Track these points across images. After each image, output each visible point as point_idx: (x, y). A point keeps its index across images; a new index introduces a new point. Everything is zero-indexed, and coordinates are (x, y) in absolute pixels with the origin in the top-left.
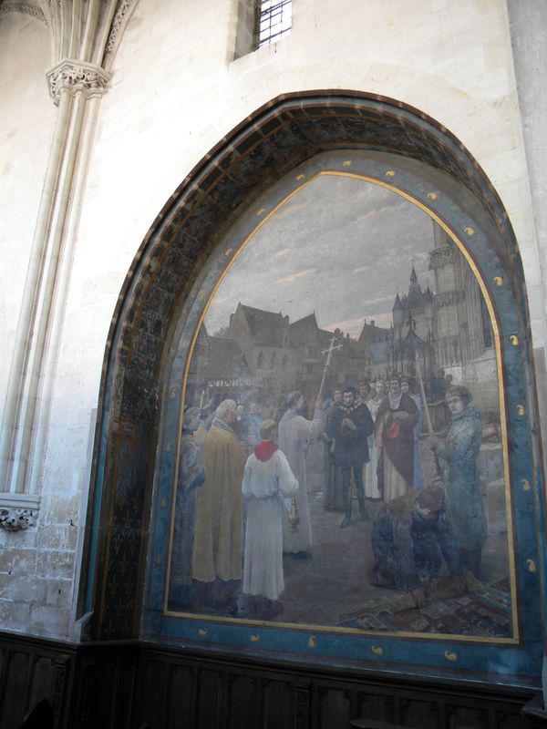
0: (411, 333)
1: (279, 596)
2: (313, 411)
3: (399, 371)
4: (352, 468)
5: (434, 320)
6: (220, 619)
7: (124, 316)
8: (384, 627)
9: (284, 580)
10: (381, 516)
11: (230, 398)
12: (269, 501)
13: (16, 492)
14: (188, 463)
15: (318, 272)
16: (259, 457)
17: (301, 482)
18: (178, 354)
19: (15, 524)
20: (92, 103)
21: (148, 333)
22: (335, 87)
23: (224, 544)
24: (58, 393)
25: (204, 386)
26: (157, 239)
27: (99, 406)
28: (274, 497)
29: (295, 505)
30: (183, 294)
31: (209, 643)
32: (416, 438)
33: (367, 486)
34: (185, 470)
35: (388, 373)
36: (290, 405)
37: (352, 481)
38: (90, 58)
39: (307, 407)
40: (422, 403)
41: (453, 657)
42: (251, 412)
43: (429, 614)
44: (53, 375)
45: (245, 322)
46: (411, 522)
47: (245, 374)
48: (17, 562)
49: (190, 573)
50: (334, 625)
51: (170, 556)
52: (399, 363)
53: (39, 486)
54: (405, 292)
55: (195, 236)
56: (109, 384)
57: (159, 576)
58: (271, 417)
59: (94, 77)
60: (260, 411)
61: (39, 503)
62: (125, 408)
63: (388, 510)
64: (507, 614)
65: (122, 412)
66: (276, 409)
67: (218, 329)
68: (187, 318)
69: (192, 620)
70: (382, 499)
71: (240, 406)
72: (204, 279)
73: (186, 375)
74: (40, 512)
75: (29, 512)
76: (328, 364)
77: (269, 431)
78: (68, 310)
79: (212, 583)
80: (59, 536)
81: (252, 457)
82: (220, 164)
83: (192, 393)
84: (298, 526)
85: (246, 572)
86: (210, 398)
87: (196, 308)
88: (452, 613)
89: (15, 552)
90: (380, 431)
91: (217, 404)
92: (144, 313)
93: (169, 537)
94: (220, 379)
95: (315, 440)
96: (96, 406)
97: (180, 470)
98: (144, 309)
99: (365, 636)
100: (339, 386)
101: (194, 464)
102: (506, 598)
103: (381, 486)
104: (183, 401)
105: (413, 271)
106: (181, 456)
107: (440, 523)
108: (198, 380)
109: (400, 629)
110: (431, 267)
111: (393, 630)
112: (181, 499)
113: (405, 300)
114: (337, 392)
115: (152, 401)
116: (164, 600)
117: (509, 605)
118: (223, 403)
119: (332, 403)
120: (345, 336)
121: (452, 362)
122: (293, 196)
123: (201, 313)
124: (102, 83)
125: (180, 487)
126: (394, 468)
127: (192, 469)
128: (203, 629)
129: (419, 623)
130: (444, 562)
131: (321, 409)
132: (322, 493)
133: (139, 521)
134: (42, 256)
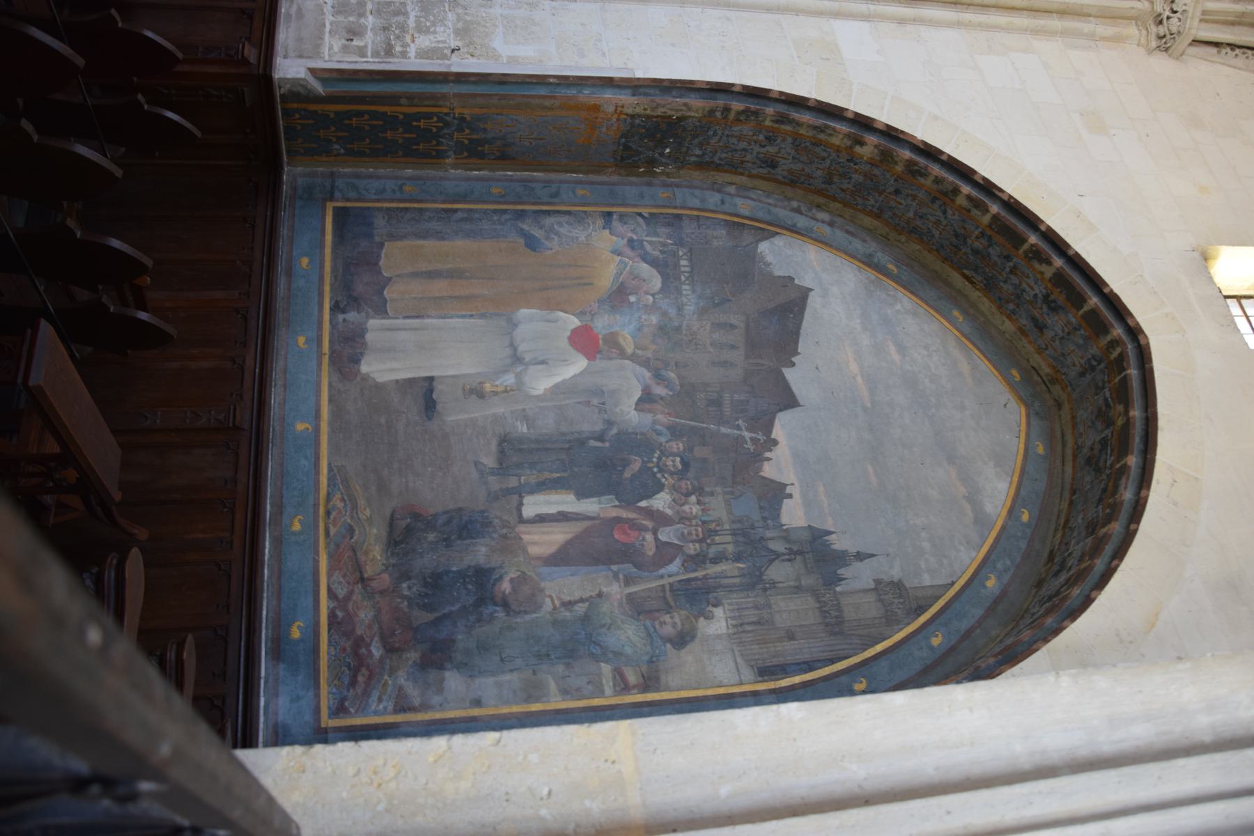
0: (777, 556)
1: (367, 374)
2: (650, 411)
3: (717, 538)
4: (565, 474)
5: (798, 589)
6: (327, 288)
7: (782, 108)
8: (333, 531)
9: (391, 381)
10: (496, 520)
11: (663, 283)
12: (508, 351)
14: (560, 224)
16: (574, 332)
17: (538, 398)
18: (727, 199)
20: (1132, 30)
21: (757, 149)
22: (1161, 422)
23: (440, 287)
25: (680, 243)
26: (907, 154)
28: (517, 359)
29: (506, 391)
30: (821, 200)
31: (289, 274)
32: (614, 568)
33: (540, 498)
34: (548, 221)
35: (712, 521)
36: (658, 377)
37: (547, 475)
38: (1207, 18)
39: (655, 401)
40: (670, 576)
41: (296, 634)
42: (644, 317)
43: (354, 598)
46: (488, 566)
49: (392, 237)
50: (328, 458)
51: (416, 205)
52: (729, 538)
54: (839, 543)
55: (916, 214)
57: (384, 190)
58: (637, 347)
59: (1174, 30)
60: (646, 330)
62: (637, 121)
63: (505, 531)
64: (362, 710)
65: (633, 116)
66: (649, 354)
67: (769, 258)
68: (784, 208)
69: (322, 246)
70: (522, 520)
71: (650, 298)
72: (848, 232)
73: (695, 213)
76: (724, 430)
79: (381, 273)
80: (435, 32)
81: (574, 322)
82: (1032, 245)
83: (669, 225)
84: (473, 397)
85: (400, 322)
87: (802, 222)
88: (359, 632)
90: (625, 514)
91: (654, 263)
92: (790, 140)
93: (444, 202)
94: (692, 266)
95: (606, 416)
96: (640, 74)
97: (548, 213)
98: (795, 140)
99: (316, 505)
100: (690, 449)
101: (557, 234)
102: (385, 708)
103: (541, 519)
105: (872, 556)
107: (491, 608)
108: (689, 228)
109: (330, 556)
110: (878, 582)
111: (327, 545)
112: (507, 216)
113: (827, 545)
114: (681, 446)
115: (652, 162)
117: (376, 713)
118: (654, 272)
119: (663, 439)
120: (767, 455)
121: (732, 618)
122: (984, 365)
123: (793, 230)
124: (1165, 44)
126: (569, 536)
129: (340, 583)
130: (431, 616)
131: (655, 422)
132: (525, 430)
133: (466, 154)
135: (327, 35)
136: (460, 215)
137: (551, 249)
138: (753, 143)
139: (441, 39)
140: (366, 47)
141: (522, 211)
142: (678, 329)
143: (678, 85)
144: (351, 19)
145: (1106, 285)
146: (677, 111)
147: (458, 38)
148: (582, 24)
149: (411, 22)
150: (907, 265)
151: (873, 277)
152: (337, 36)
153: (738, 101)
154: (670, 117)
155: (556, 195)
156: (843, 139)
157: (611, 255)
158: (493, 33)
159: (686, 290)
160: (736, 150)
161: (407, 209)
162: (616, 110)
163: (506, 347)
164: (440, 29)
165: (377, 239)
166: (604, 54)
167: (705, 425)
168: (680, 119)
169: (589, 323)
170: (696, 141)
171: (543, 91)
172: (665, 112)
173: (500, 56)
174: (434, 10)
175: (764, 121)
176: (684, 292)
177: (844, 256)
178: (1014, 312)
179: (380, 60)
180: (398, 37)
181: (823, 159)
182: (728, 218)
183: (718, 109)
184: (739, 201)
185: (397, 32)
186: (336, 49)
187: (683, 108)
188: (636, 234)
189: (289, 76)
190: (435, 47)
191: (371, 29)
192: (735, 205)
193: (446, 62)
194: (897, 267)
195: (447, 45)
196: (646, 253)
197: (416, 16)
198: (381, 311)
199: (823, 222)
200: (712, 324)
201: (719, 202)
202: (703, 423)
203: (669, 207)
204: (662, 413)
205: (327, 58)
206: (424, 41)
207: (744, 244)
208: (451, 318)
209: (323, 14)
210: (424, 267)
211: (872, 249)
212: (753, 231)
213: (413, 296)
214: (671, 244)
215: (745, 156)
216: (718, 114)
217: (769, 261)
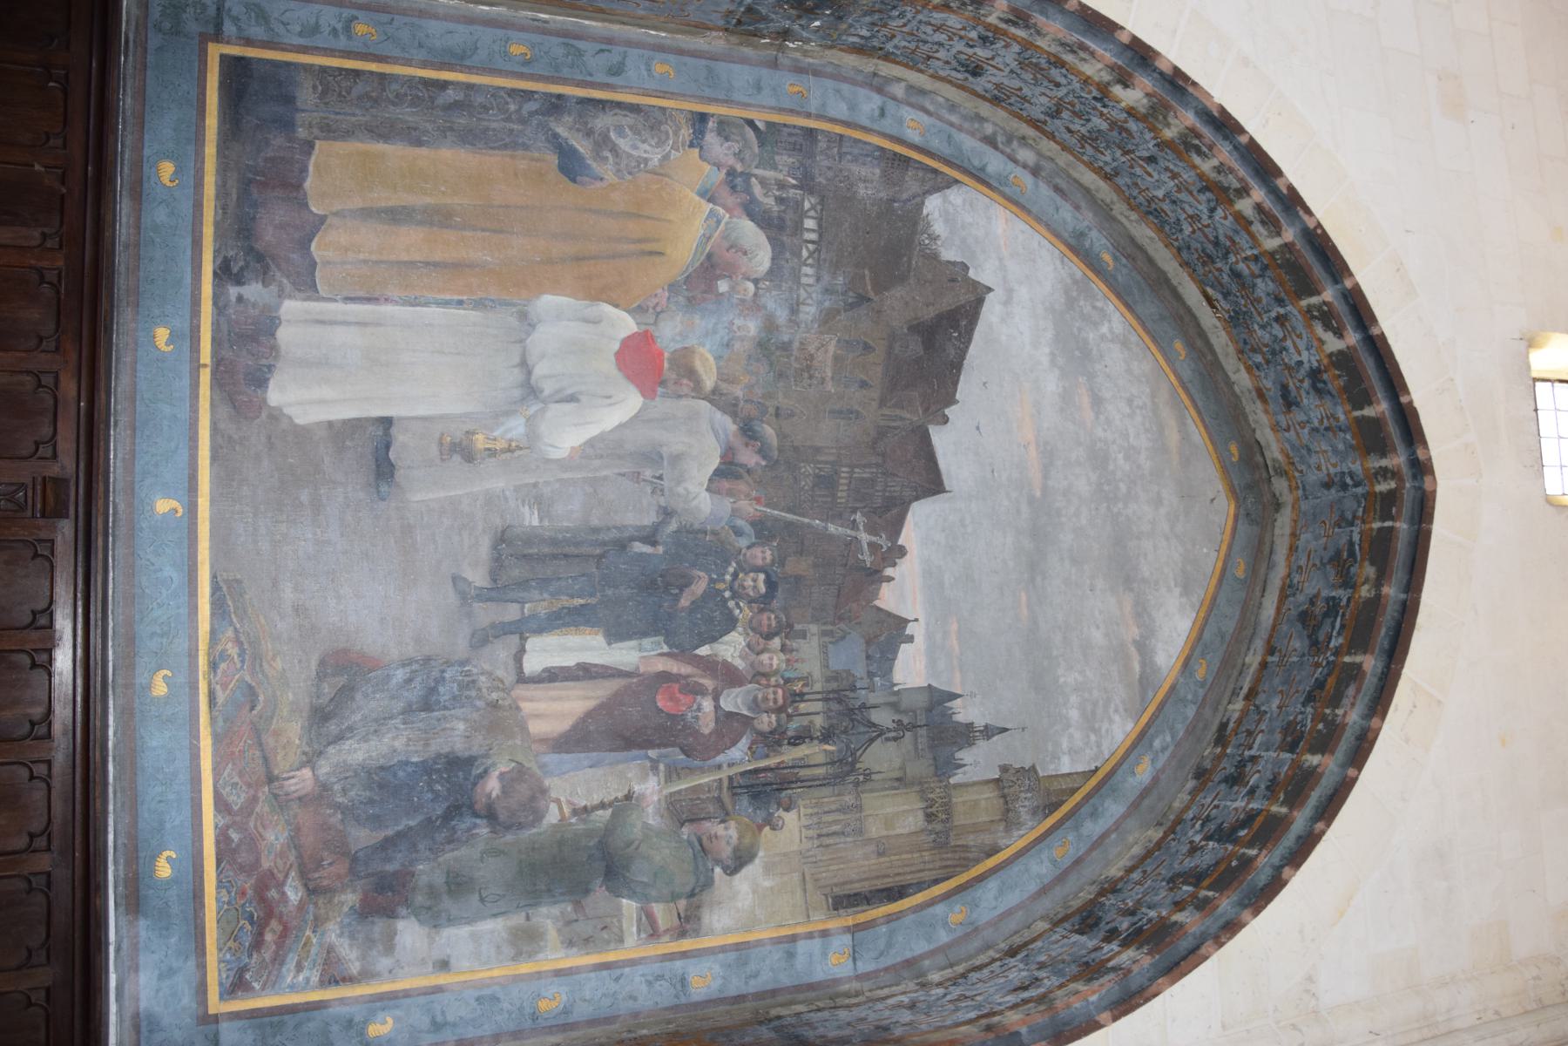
0: (879, 732)
1: (279, 409)
2: (730, 493)
3: (802, 705)
4: (592, 601)
5: (901, 781)
6: (208, 231)
8: (221, 697)
9: (318, 424)
10: (483, 678)
12: (517, 375)
14: (620, 130)
15: (1031, 500)
16: (626, 343)
17: (563, 464)
18: (891, 106)
22: (1422, 618)
23: (409, 241)
25: (807, 184)
28: (530, 391)
29: (509, 450)
31: (137, 194)
32: (652, 753)
33: (551, 640)
34: (602, 122)
35: (800, 679)
36: (748, 431)
37: (565, 601)
39: (738, 477)
40: (730, 765)
41: (164, 870)
42: (738, 322)
43: (258, 809)
45: (947, 303)
46: (467, 754)
47: (827, 304)
49: (330, 131)
50: (212, 567)
51: (373, 67)
52: (818, 706)
54: (966, 712)
55: (1167, 195)
57: (315, 29)
58: (722, 377)
60: (737, 345)
63: (494, 696)
64: (271, 985)
66: (739, 392)
67: (938, 227)
68: (972, 134)
69: (199, 141)
70: (522, 679)
71: (751, 286)
73: (838, 129)
76: (832, 528)
77: (691, 373)
79: (306, 205)
81: (627, 325)
83: (795, 148)
84: (457, 458)
85: (337, 308)
86: (780, 200)
88: (266, 864)
90: (674, 667)
91: (765, 221)
93: (424, 65)
94: (821, 230)
95: (662, 501)
97: (602, 105)
99: (193, 655)
100: (781, 561)
101: (614, 150)
102: (308, 980)
104: (776, 118)
105: (1005, 730)
106: (635, 109)
107: (469, 821)
109: (217, 738)
110: (1004, 769)
111: (213, 720)
112: (532, 106)
113: (947, 715)
114: (768, 553)
116: (249, 42)
117: (293, 988)
118: (761, 238)
119: (743, 543)
120: (889, 572)
121: (808, 827)
122: (1197, 434)
123: (980, 177)
125: (556, 105)
126: (591, 704)
127: (603, 143)
128: (178, 172)
129: (234, 785)
130: (381, 835)
131: (735, 512)
132: (536, 522)
136: (451, 95)
137: (602, 179)
138: (956, 39)
141: (559, 97)
142: (785, 347)
145: (1407, 392)
150: (1128, 257)
151: (1079, 274)
155: (617, 70)
156: (1101, 70)
157: (697, 198)
159: (806, 275)
160: (926, 42)
161: (357, 73)
163: (515, 367)
165: (301, 133)
167: (806, 520)
169: (652, 328)
170: (868, 19)
176: (804, 280)
177: (1044, 231)
178: (1258, 367)
181: (1058, 85)
182: (887, 144)
184: (908, 114)
188: (742, 160)
192: (901, 121)
194: (1115, 259)
196: (753, 200)
198: (306, 284)
199: (1025, 166)
200: (839, 341)
201: (877, 113)
202: (803, 515)
203: (798, 113)
204: (747, 496)
207: (905, 196)
208: (426, 304)
210: (384, 198)
211: (1086, 223)
212: (921, 174)
213: (361, 256)
214: (794, 187)
215: (937, 51)
217: (937, 233)
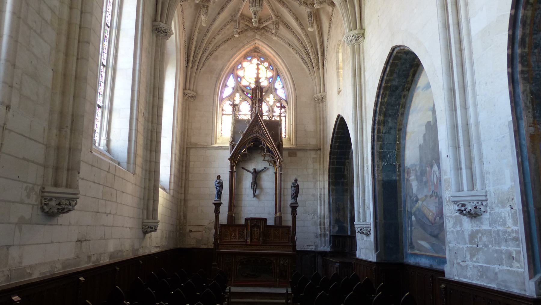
7: (517, 45)
13: (468, 191)
19: (472, 212)
24: (482, 116)
27: (513, 118)
44: (475, 105)
48: (480, 238)
53: (483, 184)
56: (517, 100)
61: (486, 196)
62: (537, 114)
65: (535, 117)
74: (488, 202)
75: (480, 203)
78: (475, 56)
80: (505, 217)
89: (478, 232)
92: (535, 36)
96: (510, 118)
98: (534, 34)
134: (446, 27)
135: (512, 269)
139: (507, 215)
140: (515, 250)
143: (513, 99)
144: (504, 256)
146: (527, 96)
147: (506, 206)
148: (492, 149)
149: (501, 228)
152: (512, 264)
153: (517, 67)
154: (531, 99)
158: (501, 190)
162: (532, 126)
164: (503, 215)
166: (504, 137)
168: (532, 93)
171: (527, 164)
172: (530, 102)
173: (511, 186)
174: (495, 218)
175: (526, 52)
179: (521, 244)
180: (509, 235)
183: (523, 76)
185: (507, 235)
186: (518, 265)
187: (525, 93)
189: (534, 290)
190: (512, 217)
191: (507, 247)
193: (518, 211)
195: (510, 211)
197: (499, 226)
205: (523, 270)
206: (510, 222)
209: (503, 270)
216: (526, 76)
